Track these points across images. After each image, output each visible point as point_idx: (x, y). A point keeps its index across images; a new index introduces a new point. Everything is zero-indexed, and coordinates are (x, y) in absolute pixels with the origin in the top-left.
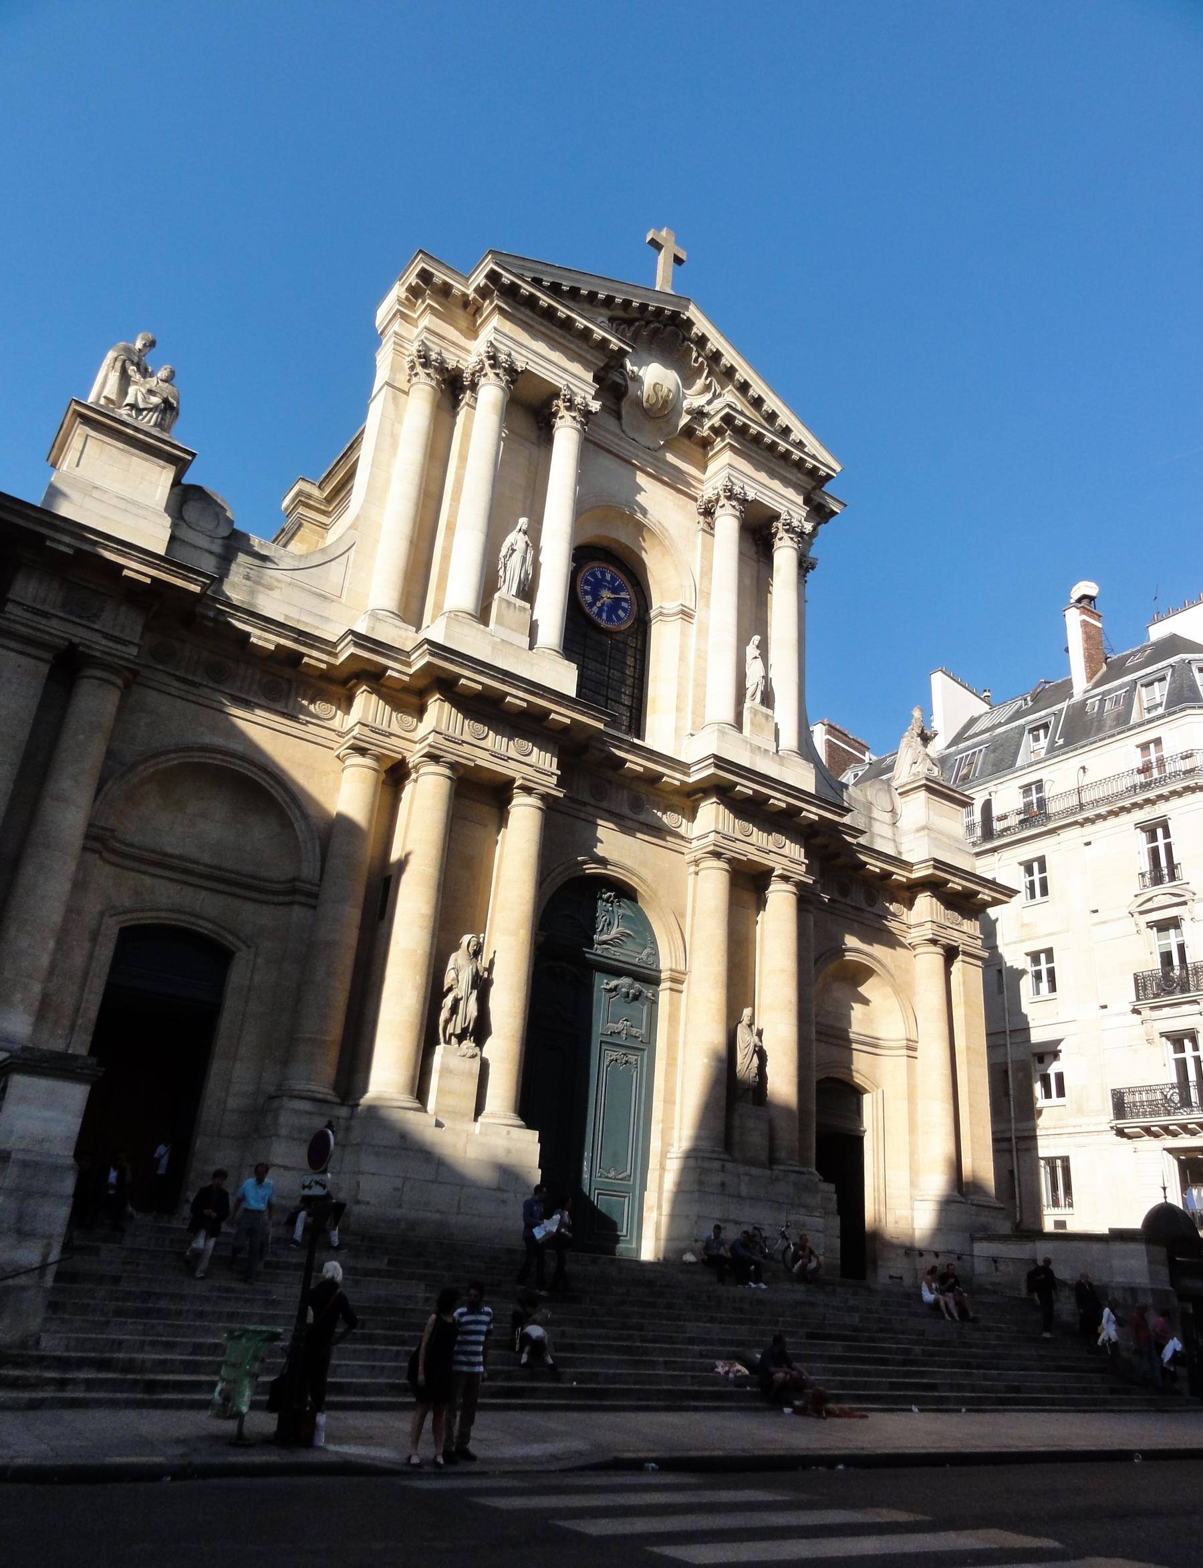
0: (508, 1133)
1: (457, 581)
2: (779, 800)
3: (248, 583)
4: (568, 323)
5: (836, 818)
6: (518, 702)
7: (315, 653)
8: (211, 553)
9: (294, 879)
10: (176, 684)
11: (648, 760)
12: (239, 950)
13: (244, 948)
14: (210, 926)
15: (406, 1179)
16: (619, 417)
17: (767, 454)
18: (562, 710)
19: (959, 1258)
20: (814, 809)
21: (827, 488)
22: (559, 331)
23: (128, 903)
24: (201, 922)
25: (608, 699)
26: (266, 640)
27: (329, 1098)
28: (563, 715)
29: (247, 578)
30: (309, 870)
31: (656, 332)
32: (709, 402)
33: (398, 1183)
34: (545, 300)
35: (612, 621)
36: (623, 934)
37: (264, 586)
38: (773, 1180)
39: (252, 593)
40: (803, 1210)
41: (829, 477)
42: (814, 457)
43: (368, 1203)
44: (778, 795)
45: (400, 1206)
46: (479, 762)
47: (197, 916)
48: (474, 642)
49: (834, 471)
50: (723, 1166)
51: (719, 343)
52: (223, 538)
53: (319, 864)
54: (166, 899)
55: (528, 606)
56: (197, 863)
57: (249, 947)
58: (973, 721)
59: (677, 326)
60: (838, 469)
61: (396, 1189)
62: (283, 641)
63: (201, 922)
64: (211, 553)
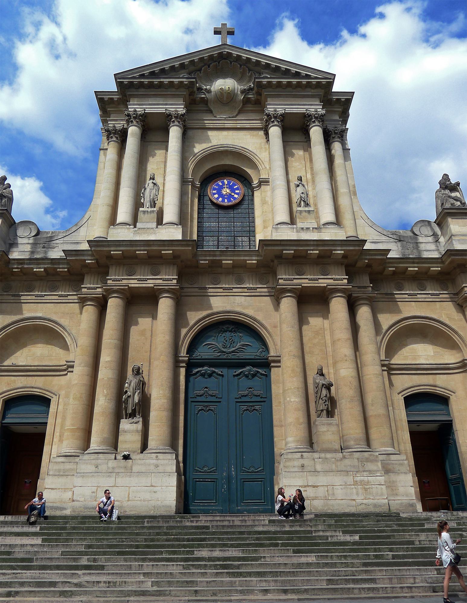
1: (124, 214)
3: (44, 249)
4: (161, 85)
10: (12, 298)
11: (233, 256)
17: (289, 89)
18: (166, 248)
22: (159, 90)
25: (234, 236)
29: (44, 247)
33: (94, 489)
35: (231, 201)
36: (243, 345)
37: (51, 248)
38: (344, 457)
39: (46, 252)
40: (365, 473)
44: (312, 248)
49: (330, 79)
50: (302, 455)
52: (34, 236)
59: (225, 59)
61: (93, 492)
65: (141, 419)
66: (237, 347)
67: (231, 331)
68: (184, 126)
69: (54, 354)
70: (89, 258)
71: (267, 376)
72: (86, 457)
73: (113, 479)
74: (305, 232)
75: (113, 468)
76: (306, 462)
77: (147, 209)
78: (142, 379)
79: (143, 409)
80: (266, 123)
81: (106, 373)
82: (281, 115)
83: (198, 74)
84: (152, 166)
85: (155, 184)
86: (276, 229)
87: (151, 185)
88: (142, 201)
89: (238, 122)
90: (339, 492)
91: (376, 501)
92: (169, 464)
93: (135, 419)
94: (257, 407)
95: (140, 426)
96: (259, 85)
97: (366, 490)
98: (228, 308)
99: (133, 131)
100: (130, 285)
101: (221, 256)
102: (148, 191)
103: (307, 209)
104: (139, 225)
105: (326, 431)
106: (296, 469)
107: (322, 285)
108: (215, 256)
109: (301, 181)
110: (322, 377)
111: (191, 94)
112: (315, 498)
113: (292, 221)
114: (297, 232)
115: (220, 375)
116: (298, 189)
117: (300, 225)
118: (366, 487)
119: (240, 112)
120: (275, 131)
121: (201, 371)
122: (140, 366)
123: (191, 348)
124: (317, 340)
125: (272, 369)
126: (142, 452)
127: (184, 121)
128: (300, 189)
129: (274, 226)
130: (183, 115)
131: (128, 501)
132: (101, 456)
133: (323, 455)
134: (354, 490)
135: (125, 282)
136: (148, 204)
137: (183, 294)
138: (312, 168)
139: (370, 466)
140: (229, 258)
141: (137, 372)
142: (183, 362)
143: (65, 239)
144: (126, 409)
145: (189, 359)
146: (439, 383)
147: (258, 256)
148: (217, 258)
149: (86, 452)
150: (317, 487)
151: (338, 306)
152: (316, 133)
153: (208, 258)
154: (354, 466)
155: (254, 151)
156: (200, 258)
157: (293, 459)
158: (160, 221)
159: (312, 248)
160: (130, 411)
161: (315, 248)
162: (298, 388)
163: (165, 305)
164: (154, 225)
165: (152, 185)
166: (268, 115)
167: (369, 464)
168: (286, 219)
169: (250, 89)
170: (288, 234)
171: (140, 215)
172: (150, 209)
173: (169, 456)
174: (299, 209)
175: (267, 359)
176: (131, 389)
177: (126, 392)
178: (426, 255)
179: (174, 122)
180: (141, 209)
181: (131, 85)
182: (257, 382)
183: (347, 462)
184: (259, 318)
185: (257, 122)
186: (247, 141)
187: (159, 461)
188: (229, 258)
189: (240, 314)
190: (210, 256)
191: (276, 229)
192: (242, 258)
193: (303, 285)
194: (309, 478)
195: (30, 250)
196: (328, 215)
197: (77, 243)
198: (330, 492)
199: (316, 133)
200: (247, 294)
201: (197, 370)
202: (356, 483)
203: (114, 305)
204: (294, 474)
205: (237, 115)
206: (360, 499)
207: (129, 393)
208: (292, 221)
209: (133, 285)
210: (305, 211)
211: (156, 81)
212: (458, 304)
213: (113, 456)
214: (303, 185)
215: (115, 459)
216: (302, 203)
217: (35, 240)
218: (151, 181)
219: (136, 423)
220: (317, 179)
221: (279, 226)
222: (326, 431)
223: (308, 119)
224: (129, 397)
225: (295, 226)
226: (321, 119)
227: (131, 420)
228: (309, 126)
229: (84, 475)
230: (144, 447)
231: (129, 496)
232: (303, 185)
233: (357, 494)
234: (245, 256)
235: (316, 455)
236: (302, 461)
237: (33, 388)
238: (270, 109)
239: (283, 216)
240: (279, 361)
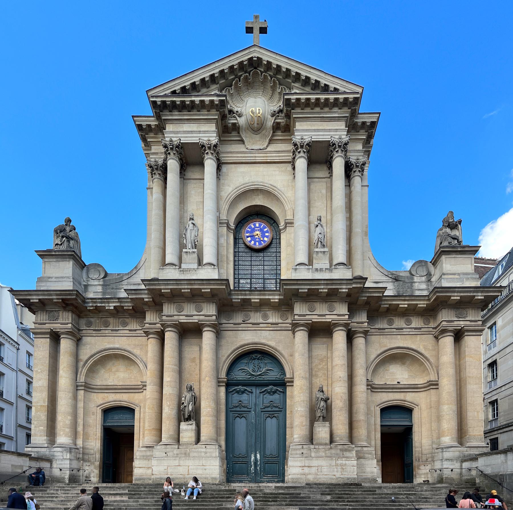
15: (168, 466)
16: (242, 141)
19: (452, 470)
38: (331, 448)
40: (344, 459)
43: (156, 475)
65: (194, 422)
68: (218, 160)
69: (133, 377)
70: (146, 296)
71: (284, 393)
72: (158, 447)
73: (177, 461)
74: (321, 272)
75: (177, 454)
76: (305, 451)
77: (189, 250)
78: (193, 394)
79: (194, 416)
80: (293, 155)
81: (169, 390)
82: (308, 144)
83: (229, 92)
84: (192, 208)
85: (194, 224)
86: (296, 269)
87: (191, 226)
88: (185, 242)
90: (325, 470)
91: (349, 476)
93: (190, 422)
95: (194, 427)
99: (173, 165)
100: (180, 321)
101: (250, 295)
102: (189, 231)
103: (322, 250)
104: (183, 266)
105: (322, 432)
106: (298, 456)
107: (328, 320)
108: (245, 295)
109: (320, 220)
110: (321, 393)
111: (223, 117)
112: (310, 474)
113: (310, 262)
114: (312, 272)
116: (317, 229)
117: (316, 266)
119: (271, 141)
122: (192, 385)
123: (228, 373)
124: (321, 366)
125: (287, 388)
126: (196, 444)
127: (218, 153)
128: (318, 230)
129: (294, 267)
130: (215, 146)
132: (168, 446)
133: (317, 447)
134: (336, 469)
135: (176, 318)
137: (222, 329)
138: (331, 207)
139: (347, 454)
140: (257, 297)
141: (190, 389)
142: (223, 382)
144: (184, 415)
145: (228, 380)
147: (280, 295)
148: (248, 297)
149: (160, 444)
150: (311, 467)
151: (339, 337)
152: (338, 164)
153: (240, 297)
154: (337, 454)
156: (234, 297)
157: (297, 449)
158: (200, 262)
160: (186, 417)
162: (304, 401)
163: (208, 337)
164: (195, 266)
166: (295, 145)
167: (347, 453)
168: (305, 260)
169: (281, 111)
170: (304, 274)
171: (184, 256)
172: (191, 251)
173: (213, 447)
174: (316, 250)
175: (284, 380)
176: (186, 402)
177: (183, 403)
179: (207, 153)
180: (184, 250)
182: (276, 396)
183: (333, 451)
184: (278, 348)
185: (286, 154)
186: (274, 177)
187: (207, 450)
188: (257, 297)
190: (242, 295)
191: (296, 269)
192: (267, 297)
193: (313, 320)
194: (306, 461)
196: (340, 256)
198: (319, 470)
199: (338, 164)
202: (337, 465)
203: (170, 337)
204: (296, 459)
205: (267, 146)
206: (338, 475)
207: (185, 404)
208: (310, 262)
209: (182, 321)
210: (321, 252)
213: (177, 447)
214: (322, 226)
215: (178, 448)
218: (191, 221)
220: (334, 219)
221: (298, 267)
222: (322, 432)
223: (332, 148)
224: (185, 407)
225: (311, 267)
226: (344, 147)
227: (187, 423)
228: (332, 157)
229: (159, 459)
230: (198, 440)
232: (322, 226)
233: (337, 472)
234: (269, 295)
235: (312, 447)
236: (302, 451)
237: (121, 401)
238: (297, 138)
239: (303, 258)
240: (293, 382)
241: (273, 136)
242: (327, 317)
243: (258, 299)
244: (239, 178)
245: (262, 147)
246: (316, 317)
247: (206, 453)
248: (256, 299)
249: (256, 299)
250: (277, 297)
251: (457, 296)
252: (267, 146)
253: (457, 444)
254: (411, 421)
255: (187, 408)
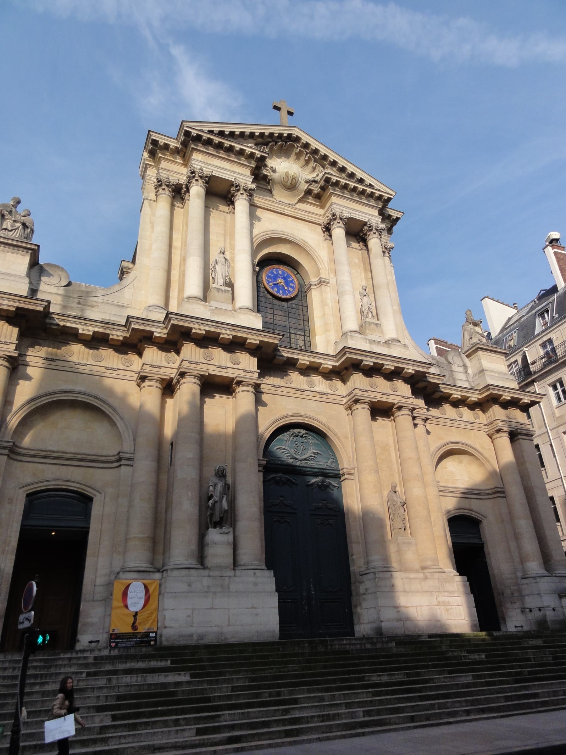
0: (255, 574)
2: (389, 365)
3: (80, 306)
4: (230, 149)
5: (425, 370)
6: (227, 337)
7: (115, 333)
8: (58, 294)
9: (119, 453)
12: (95, 495)
13: (97, 494)
14: (77, 485)
15: (193, 609)
18: (253, 337)
20: (411, 367)
21: (390, 205)
23: (29, 481)
24: (72, 484)
25: (290, 333)
26: (88, 330)
27: (147, 569)
28: (254, 339)
29: (79, 303)
30: (127, 447)
31: (282, 146)
32: (317, 176)
34: (217, 140)
37: (89, 306)
38: (426, 578)
39: (82, 310)
40: (446, 594)
41: (389, 199)
42: (379, 190)
43: (171, 627)
44: (388, 363)
45: (192, 626)
46: (211, 372)
47: (69, 481)
48: (199, 310)
49: (392, 195)
51: (316, 145)
52: (64, 286)
53: (132, 443)
54: (50, 475)
55: (229, 289)
56: (66, 453)
57: (100, 493)
58: (510, 319)
60: (394, 194)
61: (188, 616)
62: (96, 329)
63: (72, 484)
64: (58, 294)
66: (308, 455)
67: (302, 437)
75: (208, 587)
89: (297, 211)
92: (267, 581)
93: (225, 529)
94: (331, 521)
96: (327, 180)
97: (448, 610)
98: (302, 412)
108: (293, 353)
115: (294, 483)
118: (449, 607)
119: (300, 201)
120: (339, 232)
121: (276, 477)
131: (229, 625)
132: (193, 572)
135: (202, 366)
136: (221, 282)
143: (106, 298)
146: (473, 507)
148: (295, 357)
155: (314, 247)
159: (388, 363)
160: (216, 518)
161: (391, 363)
165: (224, 260)
178: (459, 383)
181: (198, 138)
189: (315, 420)
195: (61, 303)
197: (122, 306)
200: (319, 399)
201: (271, 476)
205: (296, 203)
211: (227, 143)
212: (488, 435)
216: (370, 314)
217: (66, 291)
219: (227, 533)
224: (216, 502)
231: (229, 620)
241: (303, 197)
242: (391, 396)
243: (307, 361)
244: (270, 224)
245: (291, 203)
246: (379, 395)
247: (256, 584)
248: (305, 360)
249: (305, 360)
250: (330, 363)
251: (508, 396)
252: (296, 203)
253: (545, 571)
254: (480, 538)
255: (218, 505)
